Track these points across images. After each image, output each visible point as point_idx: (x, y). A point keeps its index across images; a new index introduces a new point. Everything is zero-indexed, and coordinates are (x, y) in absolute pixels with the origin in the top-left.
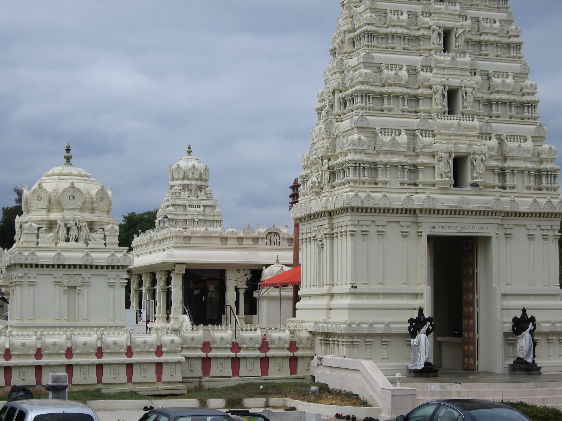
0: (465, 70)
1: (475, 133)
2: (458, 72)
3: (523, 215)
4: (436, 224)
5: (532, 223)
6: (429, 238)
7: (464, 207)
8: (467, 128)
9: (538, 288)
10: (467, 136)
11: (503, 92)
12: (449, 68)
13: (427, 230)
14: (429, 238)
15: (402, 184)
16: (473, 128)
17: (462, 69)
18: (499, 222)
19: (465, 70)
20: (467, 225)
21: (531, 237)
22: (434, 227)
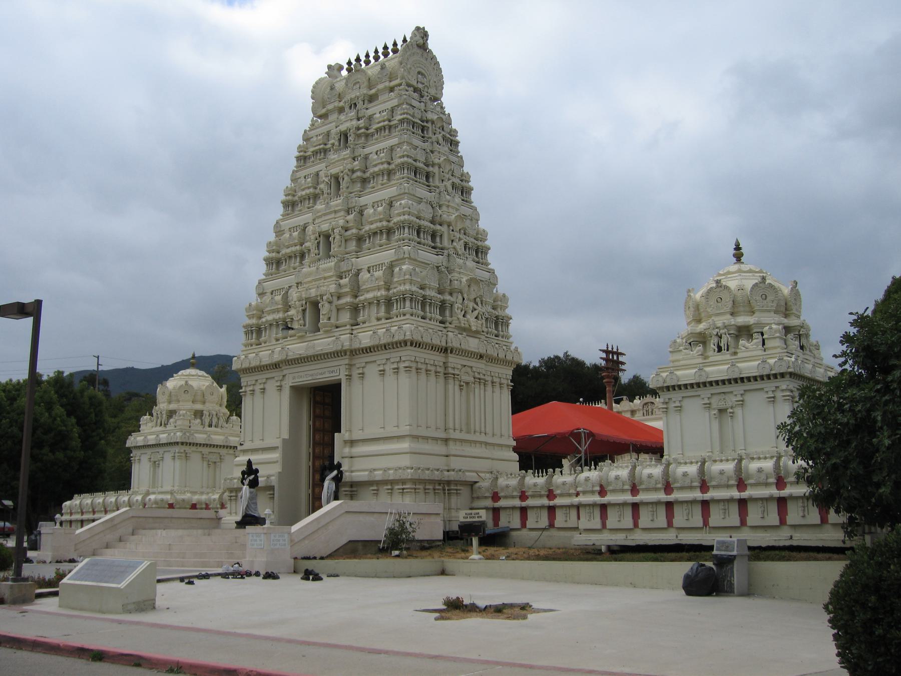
0: (339, 211)
1: (331, 274)
2: (333, 216)
3: (368, 350)
4: (296, 375)
5: (380, 357)
6: (293, 388)
7: (311, 352)
8: (324, 270)
9: (391, 431)
10: (325, 278)
11: (376, 221)
12: (325, 215)
13: (288, 383)
14: (297, 390)
15: (277, 340)
16: (329, 269)
17: (335, 212)
18: (347, 362)
19: (339, 211)
20: (320, 371)
21: (382, 373)
22: (294, 378)
